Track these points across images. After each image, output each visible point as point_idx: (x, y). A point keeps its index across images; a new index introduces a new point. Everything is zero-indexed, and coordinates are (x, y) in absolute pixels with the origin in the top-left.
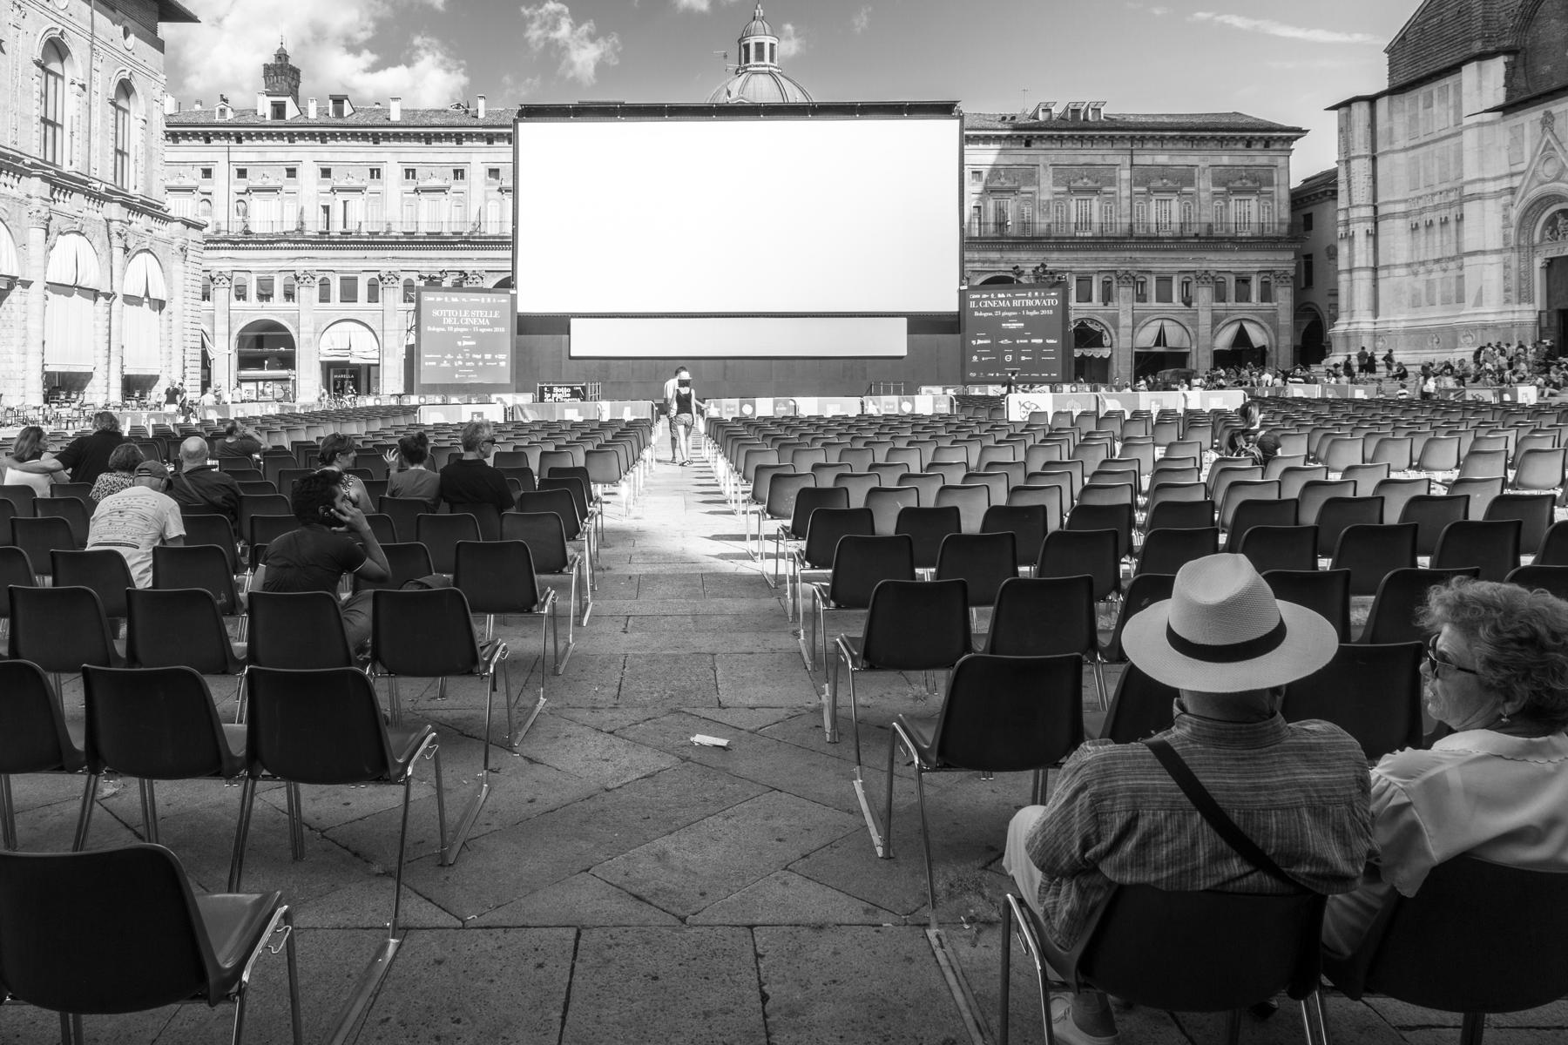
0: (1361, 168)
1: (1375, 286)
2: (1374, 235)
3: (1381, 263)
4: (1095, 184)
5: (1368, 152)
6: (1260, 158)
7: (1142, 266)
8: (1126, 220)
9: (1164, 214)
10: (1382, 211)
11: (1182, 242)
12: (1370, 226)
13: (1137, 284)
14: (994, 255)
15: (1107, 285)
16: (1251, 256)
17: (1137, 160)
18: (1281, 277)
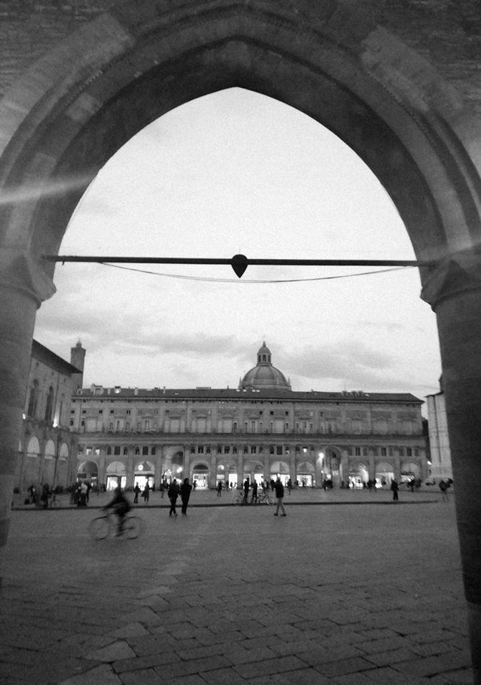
0: (432, 415)
1: (439, 452)
2: (438, 437)
3: (441, 445)
4: (360, 417)
5: (434, 412)
6: (412, 410)
7: (377, 444)
8: (370, 429)
9: (382, 427)
10: (439, 429)
11: (387, 437)
12: (436, 434)
13: (374, 449)
14: (328, 440)
15: (365, 450)
16: (411, 441)
17: (373, 410)
18: (421, 448)
